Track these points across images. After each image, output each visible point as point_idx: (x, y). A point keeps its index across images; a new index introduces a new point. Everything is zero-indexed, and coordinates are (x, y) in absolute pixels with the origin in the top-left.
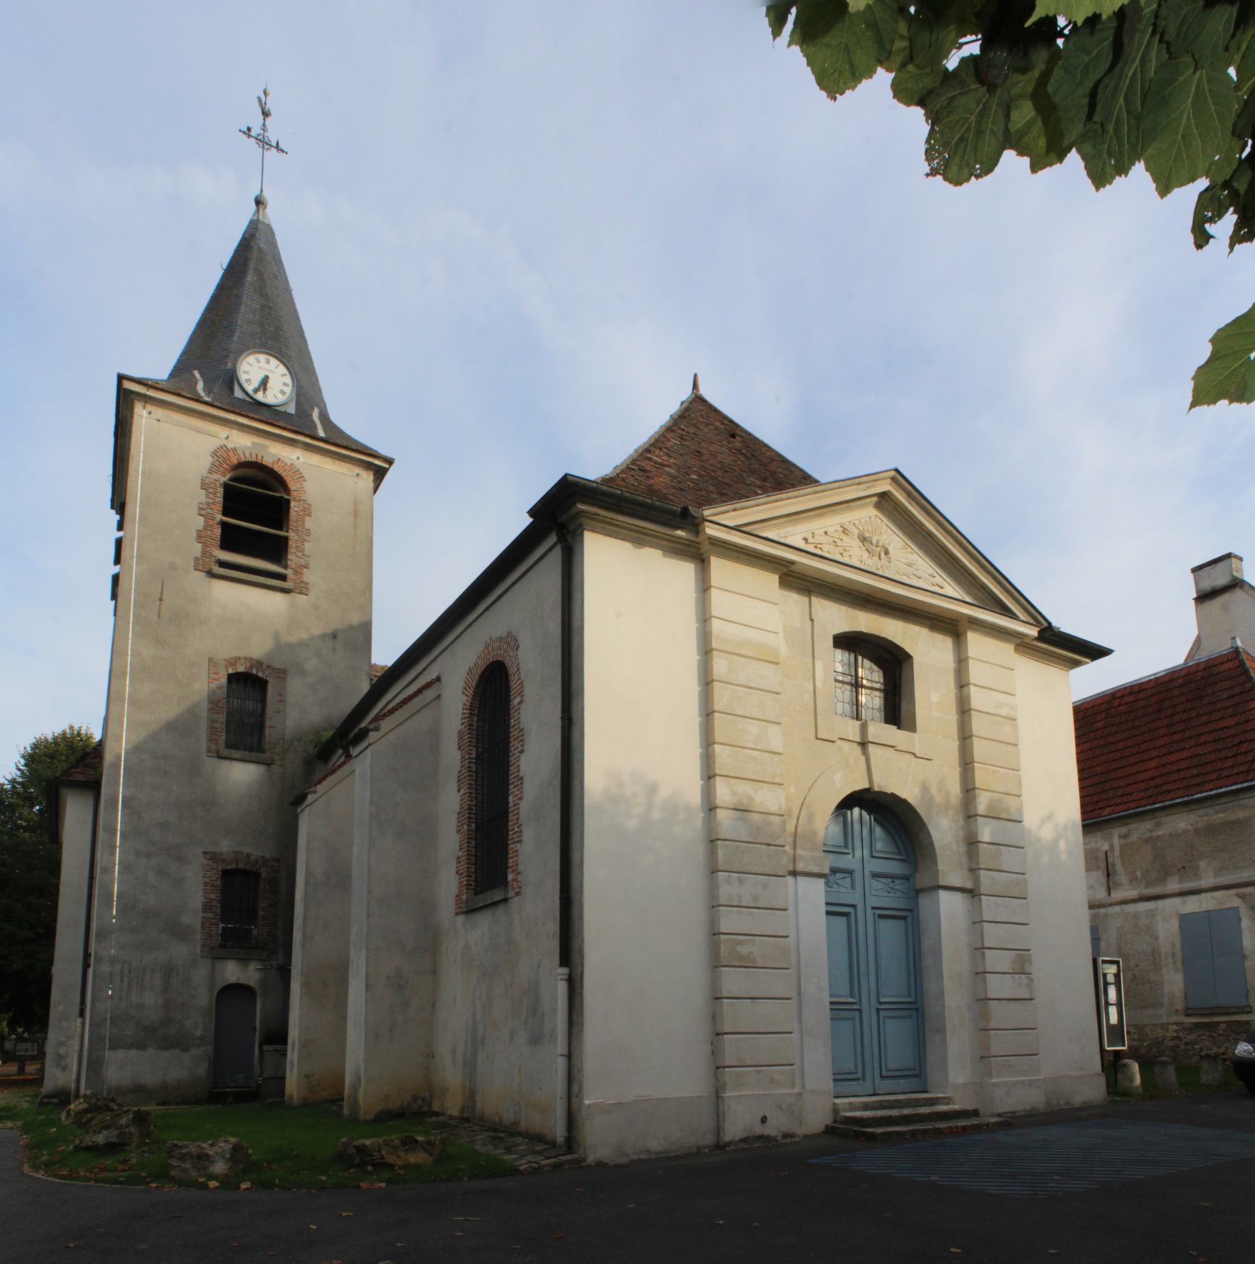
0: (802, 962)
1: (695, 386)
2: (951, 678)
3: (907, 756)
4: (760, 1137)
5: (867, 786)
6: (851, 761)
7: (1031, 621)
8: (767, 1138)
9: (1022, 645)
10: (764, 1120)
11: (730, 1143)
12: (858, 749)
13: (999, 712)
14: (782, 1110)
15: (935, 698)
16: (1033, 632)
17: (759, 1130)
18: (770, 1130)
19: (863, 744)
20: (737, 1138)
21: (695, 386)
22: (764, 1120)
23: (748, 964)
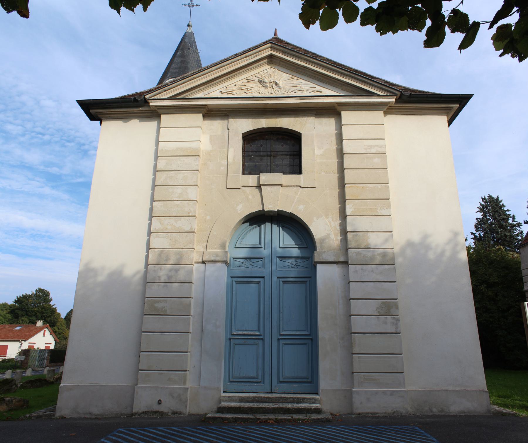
2: (334, 139)
3: (295, 188)
4: (156, 412)
5: (261, 209)
6: (250, 197)
8: (162, 413)
9: (389, 110)
10: (160, 402)
11: (136, 414)
12: (257, 190)
14: (173, 397)
15: (317, 152)
16: (392, 100)
17: (156, 408)
18: (162, 408)
19: (259, 187)
20: (141, 412)
22: (160, 402)
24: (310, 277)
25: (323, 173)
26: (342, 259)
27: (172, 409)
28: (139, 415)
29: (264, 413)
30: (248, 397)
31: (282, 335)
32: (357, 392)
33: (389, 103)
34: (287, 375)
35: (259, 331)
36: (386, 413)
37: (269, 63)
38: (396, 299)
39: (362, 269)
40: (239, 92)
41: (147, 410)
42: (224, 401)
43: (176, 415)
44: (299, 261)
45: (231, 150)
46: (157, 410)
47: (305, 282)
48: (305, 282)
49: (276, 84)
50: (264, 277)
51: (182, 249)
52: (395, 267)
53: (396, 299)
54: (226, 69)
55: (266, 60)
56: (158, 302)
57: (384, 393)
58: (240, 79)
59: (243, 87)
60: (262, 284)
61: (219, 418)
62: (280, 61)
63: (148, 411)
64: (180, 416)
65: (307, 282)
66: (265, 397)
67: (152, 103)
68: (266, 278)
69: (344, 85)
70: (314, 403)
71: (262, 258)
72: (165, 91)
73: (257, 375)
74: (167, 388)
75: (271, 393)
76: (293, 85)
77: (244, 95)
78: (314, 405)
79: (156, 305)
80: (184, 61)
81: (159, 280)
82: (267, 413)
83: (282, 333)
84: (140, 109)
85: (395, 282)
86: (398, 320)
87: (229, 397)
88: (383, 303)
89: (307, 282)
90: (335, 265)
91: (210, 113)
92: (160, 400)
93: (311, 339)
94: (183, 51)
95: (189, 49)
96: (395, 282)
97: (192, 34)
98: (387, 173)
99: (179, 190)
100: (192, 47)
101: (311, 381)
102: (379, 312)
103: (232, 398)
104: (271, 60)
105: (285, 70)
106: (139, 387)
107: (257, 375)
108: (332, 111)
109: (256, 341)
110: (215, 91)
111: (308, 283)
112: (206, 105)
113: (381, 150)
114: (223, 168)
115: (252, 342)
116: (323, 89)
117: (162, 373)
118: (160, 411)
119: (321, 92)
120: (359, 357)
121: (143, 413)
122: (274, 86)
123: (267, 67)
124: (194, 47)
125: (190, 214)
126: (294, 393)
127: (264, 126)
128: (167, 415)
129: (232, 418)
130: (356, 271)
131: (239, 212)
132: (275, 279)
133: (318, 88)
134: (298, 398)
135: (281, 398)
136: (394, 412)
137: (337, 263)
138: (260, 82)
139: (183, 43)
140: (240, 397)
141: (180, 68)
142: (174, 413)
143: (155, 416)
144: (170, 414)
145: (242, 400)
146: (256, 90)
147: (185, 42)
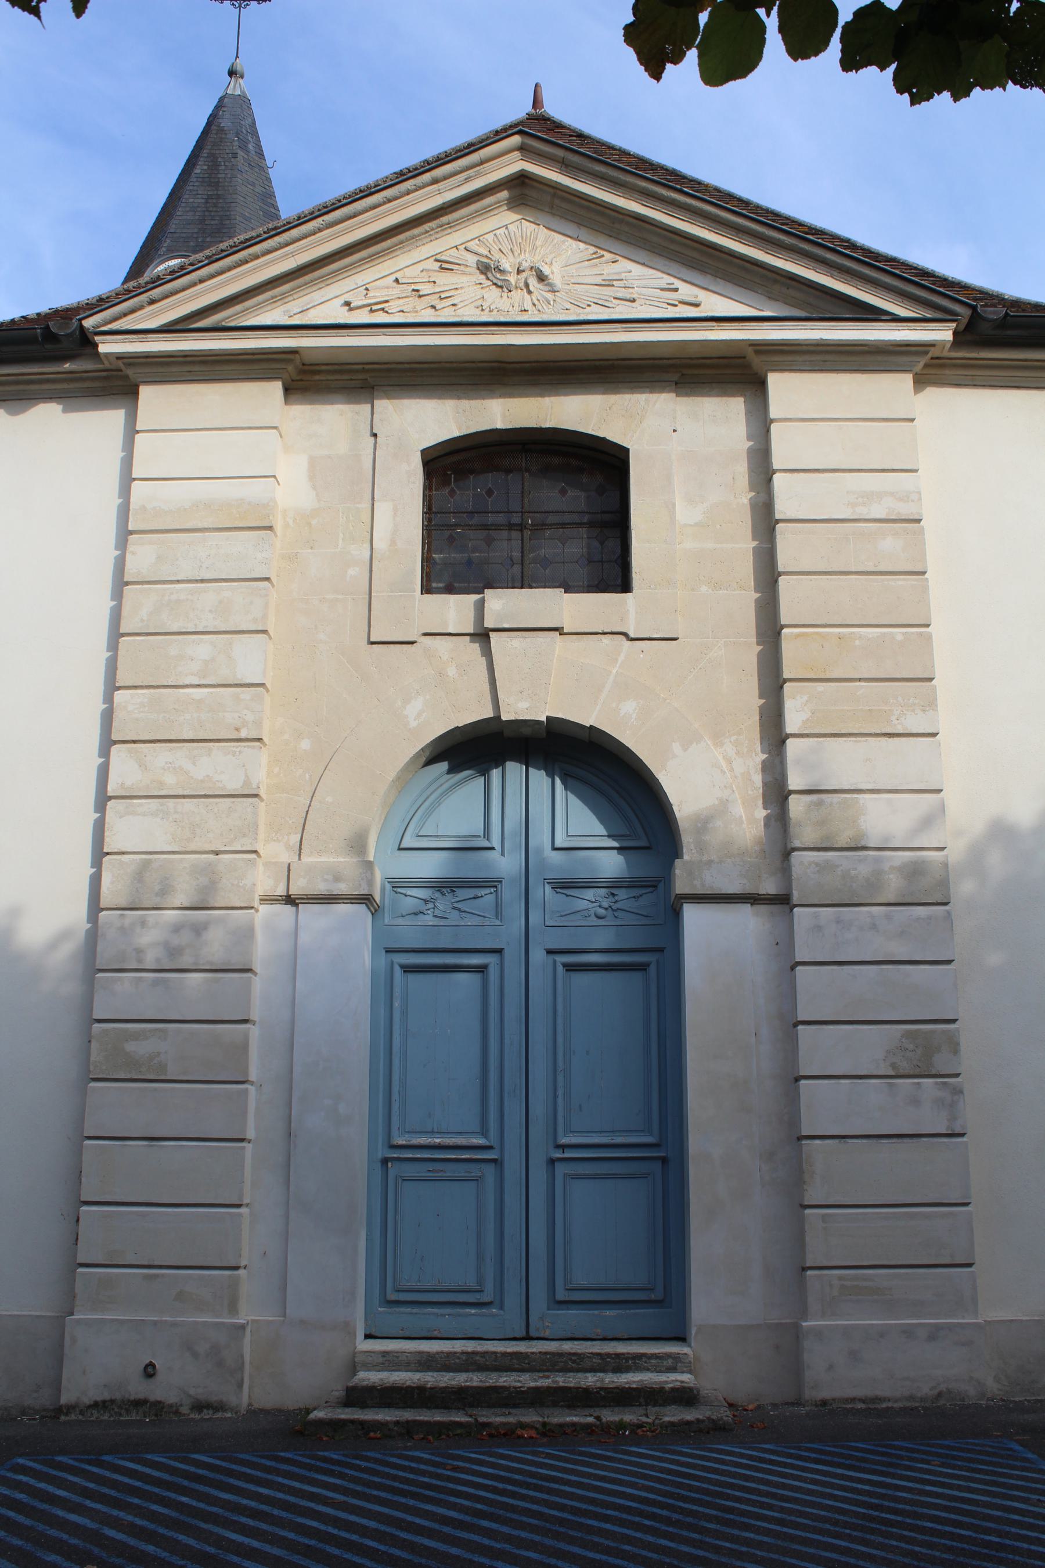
0: (297, 1069)
1: (537, 102)
2: (741, 469)
3: (606, 640)
4: (138, 1403)
5: (489, 713)
6: (452, 671)
7: (938, 315)
8: (158, 1408)
9: (931, 369)
10: (149, 1371)
11: (70, 1408)
12: (476, 646)
13: (862, 512)
14: (195, 1355)
15: (686, 514)
16: (943, 334)
17: (138, 1389)
18: (158, 1391)
19: (482, 636)
20: (87, 1401)
21: (537, 102)
22: (149, 1371)
23: (149, 1075)
24: (661, 950)
25: (704, 589)
26: (769, 887)
27: (192, 1392)
28: (82, 1413)
29: (506, 1406)
30: (449, 1355)
31: (564, 1147)
32: (819, 1333)
33: (932, 345)
34: (580, 1279)
35: (484, 1133)
36: (911, 1398)
37: (514, 204)
38: (954, 1021)
39: (838, 922)
40: (412, 302)
41: (107, 1396)
42: (368, 1367)
43: (206, 1414)
44: (622, 894)
45: (382, 509)
46: (141, 1396)
47: (642, 967)
48: (642, 967)
49: (541, 278)
50: (499, 951)
51: (217, 853)
52: (949, 912)
53: (954, 1021)
54: (363, 224)
55: (504, 194)
56: (136, 1036)
57: (908, 1332)
58: (412, 260)
59: (425, 289)
60: (493, 973)
61: (353, 1422)
62: (554, 195)
63: (112, 1401)
64: (219, 1415)
65: (648, 965)
66: (505, 1354)
67: (107, 347)
68: (506, 952)
69: (776, 281)
70: (673, 1369)
71: (493, 884)
72: (152, 302)
73: (480, 1280)
74: (174, 1324)
75: (528, 1338)
76: (598, 280)
77: (428, 316)
78: (672, 1377)
79: (130, 1047)
80: (218, 197)
81: (140, 961)
82: (515, 1406)
83: (564, 1141)
84: (67, 366)
85: (949, 962)
86: (958, 1091)
87: (385, 1354)
88: (908, 1034)
89: (648, 965)
90: (746, 909)
91: (310, 378)
92: (151, 1365)
93: (664, 1160)
94: (214, 164)
95: (235, 155)
96: (949, 962)
97: (243, 101)
98: (925, 589)
99: (202, 649)
100: (244, 147)
101: (661, 1299)
102: (893, 1066)
103: (394, 1357)
104: (522, 191)
105: (571, 228)
106: (78, 1321)
107: (480, 1280)
108: (733, 372)
109: (471, 1166)
110: (325, 303)
111: (653, 969)
112: (294, 351)
113: (905, 510)
114: (357, 572)
115: (460, 1170)
116: (702, 295)
117: (156, 1276)
118: (152, 1398)
119: (697, 305)
120: (824, 1216)
121: (95, 1405)
122: (533, 282)
123: (509, 217)
124: (251, 147)
125: (243, 734)
126: (604, 1339)
127: (500, 425)
128: (177, 1412)
129: (397, 1423)
130: (818, 928)
131: (413, 724)
132: (538, 955)
133: (686, 291)
134: (618, 1356)
135: (561, 1355)
136: (940, 1395)
137: (752, 899)
138: (484, 269)
139: (213, 136)
140: (421, 1353)
141: (202, 221)
142: (199, 1406)
143: (134, 1416)
144: (185, 1410)
145: (427, 1363)
146: (471, 299)
147: (221, 130)
